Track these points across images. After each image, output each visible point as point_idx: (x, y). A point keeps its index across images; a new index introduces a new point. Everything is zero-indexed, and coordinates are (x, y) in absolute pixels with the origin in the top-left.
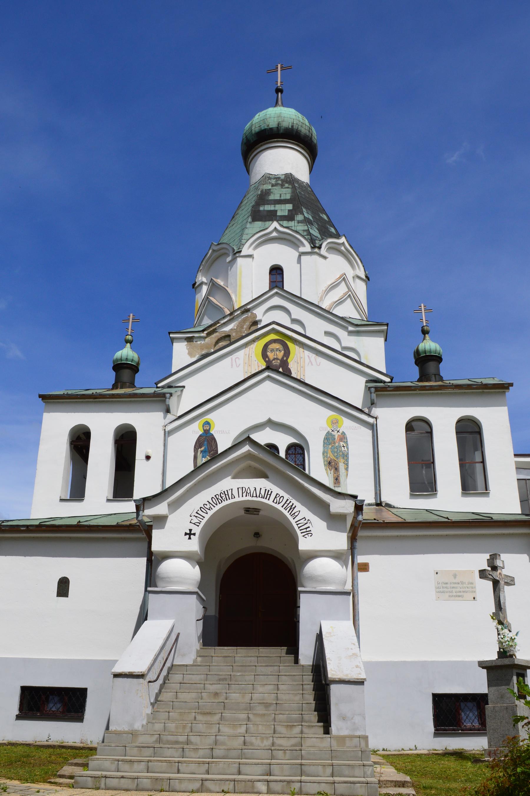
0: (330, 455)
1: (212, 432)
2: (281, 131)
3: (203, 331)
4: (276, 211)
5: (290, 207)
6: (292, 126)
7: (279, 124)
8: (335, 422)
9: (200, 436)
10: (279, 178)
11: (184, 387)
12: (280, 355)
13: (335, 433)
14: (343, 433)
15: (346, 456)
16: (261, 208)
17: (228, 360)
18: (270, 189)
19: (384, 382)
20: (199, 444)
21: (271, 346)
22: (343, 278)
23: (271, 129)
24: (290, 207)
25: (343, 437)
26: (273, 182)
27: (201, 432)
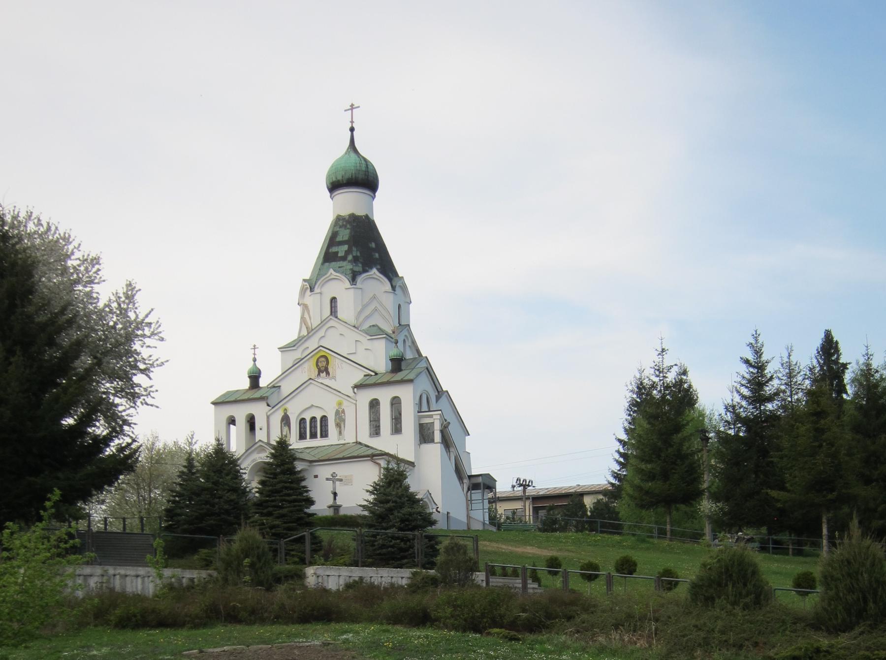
0: (337, 420)
1: (288, 413)
2: (345, 182)
3: (294, 346)
4: (337, 253)
5: (346, 247)
6: (352, 176)
7: (343, 177)
8: (340, 404)
9: (283, 416)
10: (345, 218)
11: (280, 386)
12: (324, 364)
13: (340, 410)
14: (343, 409)
15: (344, 421)
16: (330, 250)
17: (300, 369)
18: (337, 231)
19: (372, 375)
20: (282, 420)
21: (320, 360)
22: (374, 297)
23: (339, 181)
24: (346, 247)
25: (343, 411)
26: (341, 223)
27: (283, 414)
